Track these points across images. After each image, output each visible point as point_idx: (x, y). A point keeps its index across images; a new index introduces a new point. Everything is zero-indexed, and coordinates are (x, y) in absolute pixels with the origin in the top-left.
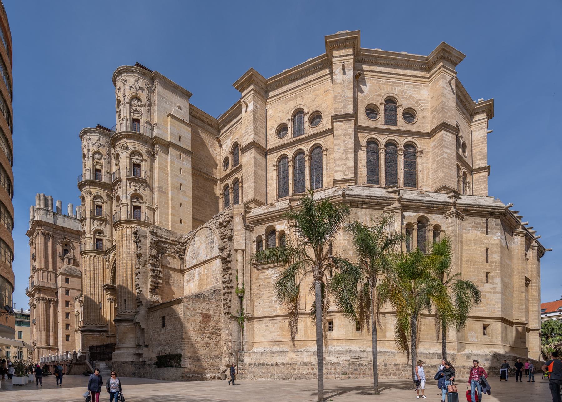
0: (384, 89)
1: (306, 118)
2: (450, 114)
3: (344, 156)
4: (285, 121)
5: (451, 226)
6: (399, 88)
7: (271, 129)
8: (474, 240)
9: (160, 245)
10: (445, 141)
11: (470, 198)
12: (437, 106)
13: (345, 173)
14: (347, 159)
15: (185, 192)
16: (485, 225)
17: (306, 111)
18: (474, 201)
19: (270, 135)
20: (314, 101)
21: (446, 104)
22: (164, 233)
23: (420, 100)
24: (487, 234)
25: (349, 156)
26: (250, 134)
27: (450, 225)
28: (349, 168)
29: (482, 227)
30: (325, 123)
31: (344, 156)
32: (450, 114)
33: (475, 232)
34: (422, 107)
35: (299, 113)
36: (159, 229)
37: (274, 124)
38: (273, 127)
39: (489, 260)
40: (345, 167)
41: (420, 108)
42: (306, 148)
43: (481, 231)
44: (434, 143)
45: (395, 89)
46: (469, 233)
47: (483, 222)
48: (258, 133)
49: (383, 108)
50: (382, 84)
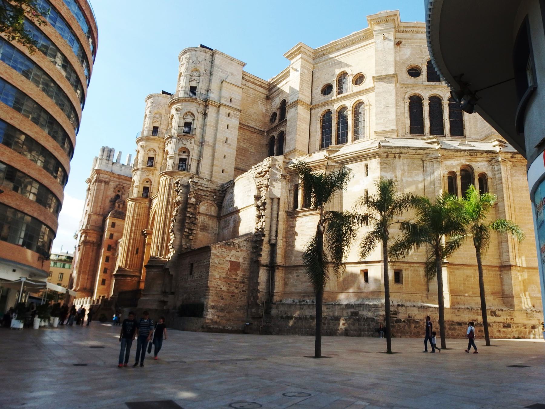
5: (498, 174)
46: (519, 180)
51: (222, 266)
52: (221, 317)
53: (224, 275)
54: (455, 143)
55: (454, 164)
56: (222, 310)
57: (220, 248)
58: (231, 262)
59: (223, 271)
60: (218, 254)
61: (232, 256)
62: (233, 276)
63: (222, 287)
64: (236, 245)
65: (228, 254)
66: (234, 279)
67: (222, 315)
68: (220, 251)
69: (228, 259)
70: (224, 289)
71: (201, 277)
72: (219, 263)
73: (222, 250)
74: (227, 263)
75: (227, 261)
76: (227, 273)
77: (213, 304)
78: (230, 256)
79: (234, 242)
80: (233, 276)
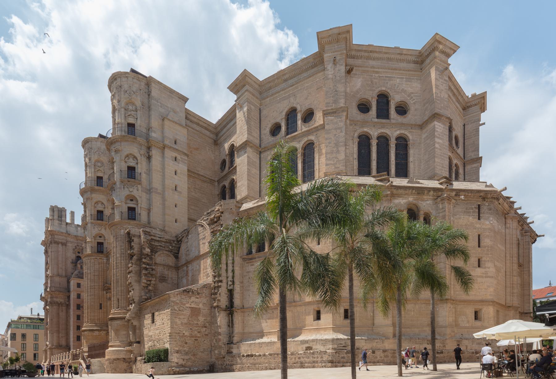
0: (376, 84)
1: (299, 116)
2: (442, 105)
3: (335, 149)
4: (278, 120)
5: (442, 212)
6: (391, 82)
7: (265, 129)
8: (466, 225)
9: (153, 243)
10: (437, 131)
11: (462, 183)
12: (429, 98)
13: (336, 166)
14: (338, 152)
15: (180, 193)
16: (477, 210)
17: (299, 108)
18: (466, 186)
19: (264, 134)
20: (307, 99)
21: (439, 95)
22: (158, 233)
23: (412, 93)
24: (479, 219)
25: (340, 149)
26: (244, 134)
27: (441, 211)
28: (340, 161)
29: (474, 212)
30: (318, 119)
31: (335, 149)
32: (442, 105)
33: (467, 217)
34: (414, 99)
35: (291, 114)
36: (153, 228)
37: (268, 124)
38: (266, 127)
39: (481, 244)
40: (336, 160)
41: (412, 101)
42: (299, 145)
43: (472, 216)
44: (426, 134)
45: (387, 83)
46: (460, 218)
47: (475, 207)
48: (252, 133)
49: (375, 102)
50: (374, 78)
51: (183, 312)
52: (186, 360)
53: (185, 321)
54: (403, 182)
55: (402, 203)
56: (187, 353)
57: (178, 296)
58: (192, 308)
59: (184, 317)
60: (178, 301)
61: (191, 302)
62: (194, 321)
63: (184, 332)
64: (195, 292)
65: (188, 301)
66: (196, 324)
67: (187, 358)
68: (179, 298)
69: (188, 305)
70: (187, 334)
71: (163, 324)
72: (180, 310)
73: (181, 297)
74: (187, 309)
75: (187, 307)
76: (189, 318)
77: (177, 349)
78: (190, 303)
79: (192, 289)
80: (194, 321)
